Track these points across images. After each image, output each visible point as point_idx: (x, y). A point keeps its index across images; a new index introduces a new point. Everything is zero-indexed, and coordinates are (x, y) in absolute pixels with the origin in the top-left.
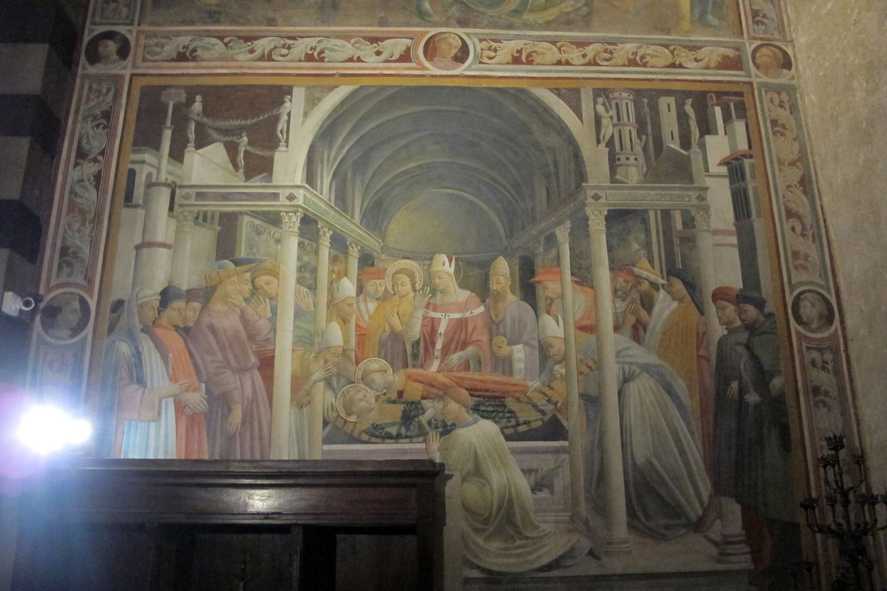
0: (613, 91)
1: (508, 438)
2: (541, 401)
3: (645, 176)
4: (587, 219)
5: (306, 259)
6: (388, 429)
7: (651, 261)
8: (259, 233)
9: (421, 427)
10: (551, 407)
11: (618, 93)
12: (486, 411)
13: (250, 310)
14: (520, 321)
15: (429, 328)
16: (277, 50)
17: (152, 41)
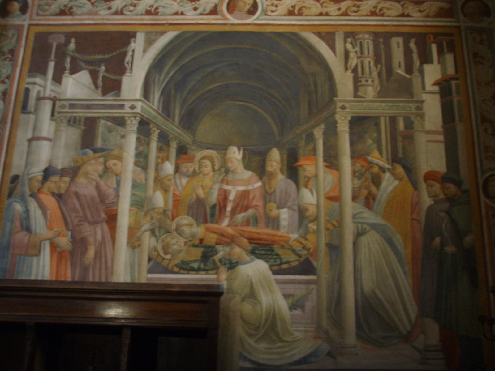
0: (358, 33)
1: (275, 273)
2: (298, 247)
3: (379, 93)
4: (335, 123)
5: (141, 148)
6: (192, 265)
7: (380, 152)
8: (110, 131)
9: (214, 263)
10: (305, 252)
11: (363, 35)
12: (260, 254)
13: (102, 183)
14: (286, 193)
15: (222, 197)
16: (127, 8)
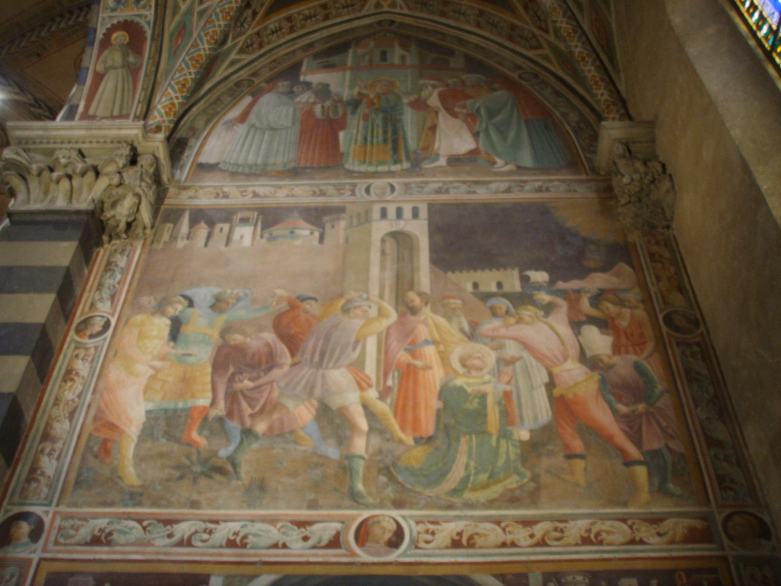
16: (197, 536)
17: (68, 524)
